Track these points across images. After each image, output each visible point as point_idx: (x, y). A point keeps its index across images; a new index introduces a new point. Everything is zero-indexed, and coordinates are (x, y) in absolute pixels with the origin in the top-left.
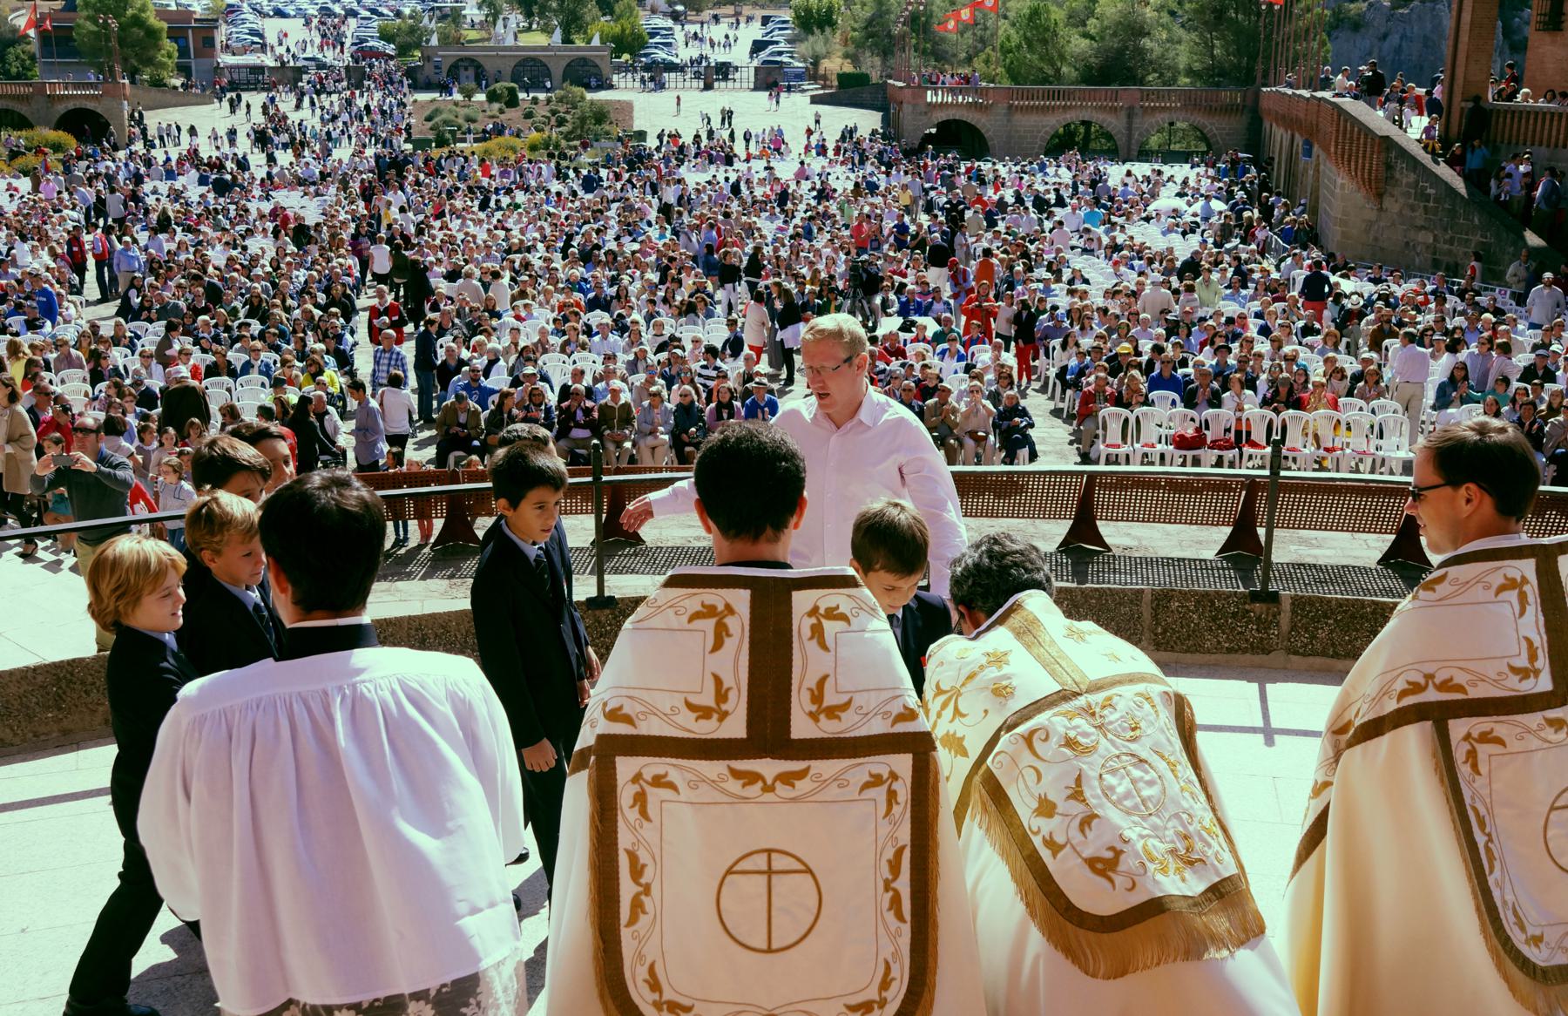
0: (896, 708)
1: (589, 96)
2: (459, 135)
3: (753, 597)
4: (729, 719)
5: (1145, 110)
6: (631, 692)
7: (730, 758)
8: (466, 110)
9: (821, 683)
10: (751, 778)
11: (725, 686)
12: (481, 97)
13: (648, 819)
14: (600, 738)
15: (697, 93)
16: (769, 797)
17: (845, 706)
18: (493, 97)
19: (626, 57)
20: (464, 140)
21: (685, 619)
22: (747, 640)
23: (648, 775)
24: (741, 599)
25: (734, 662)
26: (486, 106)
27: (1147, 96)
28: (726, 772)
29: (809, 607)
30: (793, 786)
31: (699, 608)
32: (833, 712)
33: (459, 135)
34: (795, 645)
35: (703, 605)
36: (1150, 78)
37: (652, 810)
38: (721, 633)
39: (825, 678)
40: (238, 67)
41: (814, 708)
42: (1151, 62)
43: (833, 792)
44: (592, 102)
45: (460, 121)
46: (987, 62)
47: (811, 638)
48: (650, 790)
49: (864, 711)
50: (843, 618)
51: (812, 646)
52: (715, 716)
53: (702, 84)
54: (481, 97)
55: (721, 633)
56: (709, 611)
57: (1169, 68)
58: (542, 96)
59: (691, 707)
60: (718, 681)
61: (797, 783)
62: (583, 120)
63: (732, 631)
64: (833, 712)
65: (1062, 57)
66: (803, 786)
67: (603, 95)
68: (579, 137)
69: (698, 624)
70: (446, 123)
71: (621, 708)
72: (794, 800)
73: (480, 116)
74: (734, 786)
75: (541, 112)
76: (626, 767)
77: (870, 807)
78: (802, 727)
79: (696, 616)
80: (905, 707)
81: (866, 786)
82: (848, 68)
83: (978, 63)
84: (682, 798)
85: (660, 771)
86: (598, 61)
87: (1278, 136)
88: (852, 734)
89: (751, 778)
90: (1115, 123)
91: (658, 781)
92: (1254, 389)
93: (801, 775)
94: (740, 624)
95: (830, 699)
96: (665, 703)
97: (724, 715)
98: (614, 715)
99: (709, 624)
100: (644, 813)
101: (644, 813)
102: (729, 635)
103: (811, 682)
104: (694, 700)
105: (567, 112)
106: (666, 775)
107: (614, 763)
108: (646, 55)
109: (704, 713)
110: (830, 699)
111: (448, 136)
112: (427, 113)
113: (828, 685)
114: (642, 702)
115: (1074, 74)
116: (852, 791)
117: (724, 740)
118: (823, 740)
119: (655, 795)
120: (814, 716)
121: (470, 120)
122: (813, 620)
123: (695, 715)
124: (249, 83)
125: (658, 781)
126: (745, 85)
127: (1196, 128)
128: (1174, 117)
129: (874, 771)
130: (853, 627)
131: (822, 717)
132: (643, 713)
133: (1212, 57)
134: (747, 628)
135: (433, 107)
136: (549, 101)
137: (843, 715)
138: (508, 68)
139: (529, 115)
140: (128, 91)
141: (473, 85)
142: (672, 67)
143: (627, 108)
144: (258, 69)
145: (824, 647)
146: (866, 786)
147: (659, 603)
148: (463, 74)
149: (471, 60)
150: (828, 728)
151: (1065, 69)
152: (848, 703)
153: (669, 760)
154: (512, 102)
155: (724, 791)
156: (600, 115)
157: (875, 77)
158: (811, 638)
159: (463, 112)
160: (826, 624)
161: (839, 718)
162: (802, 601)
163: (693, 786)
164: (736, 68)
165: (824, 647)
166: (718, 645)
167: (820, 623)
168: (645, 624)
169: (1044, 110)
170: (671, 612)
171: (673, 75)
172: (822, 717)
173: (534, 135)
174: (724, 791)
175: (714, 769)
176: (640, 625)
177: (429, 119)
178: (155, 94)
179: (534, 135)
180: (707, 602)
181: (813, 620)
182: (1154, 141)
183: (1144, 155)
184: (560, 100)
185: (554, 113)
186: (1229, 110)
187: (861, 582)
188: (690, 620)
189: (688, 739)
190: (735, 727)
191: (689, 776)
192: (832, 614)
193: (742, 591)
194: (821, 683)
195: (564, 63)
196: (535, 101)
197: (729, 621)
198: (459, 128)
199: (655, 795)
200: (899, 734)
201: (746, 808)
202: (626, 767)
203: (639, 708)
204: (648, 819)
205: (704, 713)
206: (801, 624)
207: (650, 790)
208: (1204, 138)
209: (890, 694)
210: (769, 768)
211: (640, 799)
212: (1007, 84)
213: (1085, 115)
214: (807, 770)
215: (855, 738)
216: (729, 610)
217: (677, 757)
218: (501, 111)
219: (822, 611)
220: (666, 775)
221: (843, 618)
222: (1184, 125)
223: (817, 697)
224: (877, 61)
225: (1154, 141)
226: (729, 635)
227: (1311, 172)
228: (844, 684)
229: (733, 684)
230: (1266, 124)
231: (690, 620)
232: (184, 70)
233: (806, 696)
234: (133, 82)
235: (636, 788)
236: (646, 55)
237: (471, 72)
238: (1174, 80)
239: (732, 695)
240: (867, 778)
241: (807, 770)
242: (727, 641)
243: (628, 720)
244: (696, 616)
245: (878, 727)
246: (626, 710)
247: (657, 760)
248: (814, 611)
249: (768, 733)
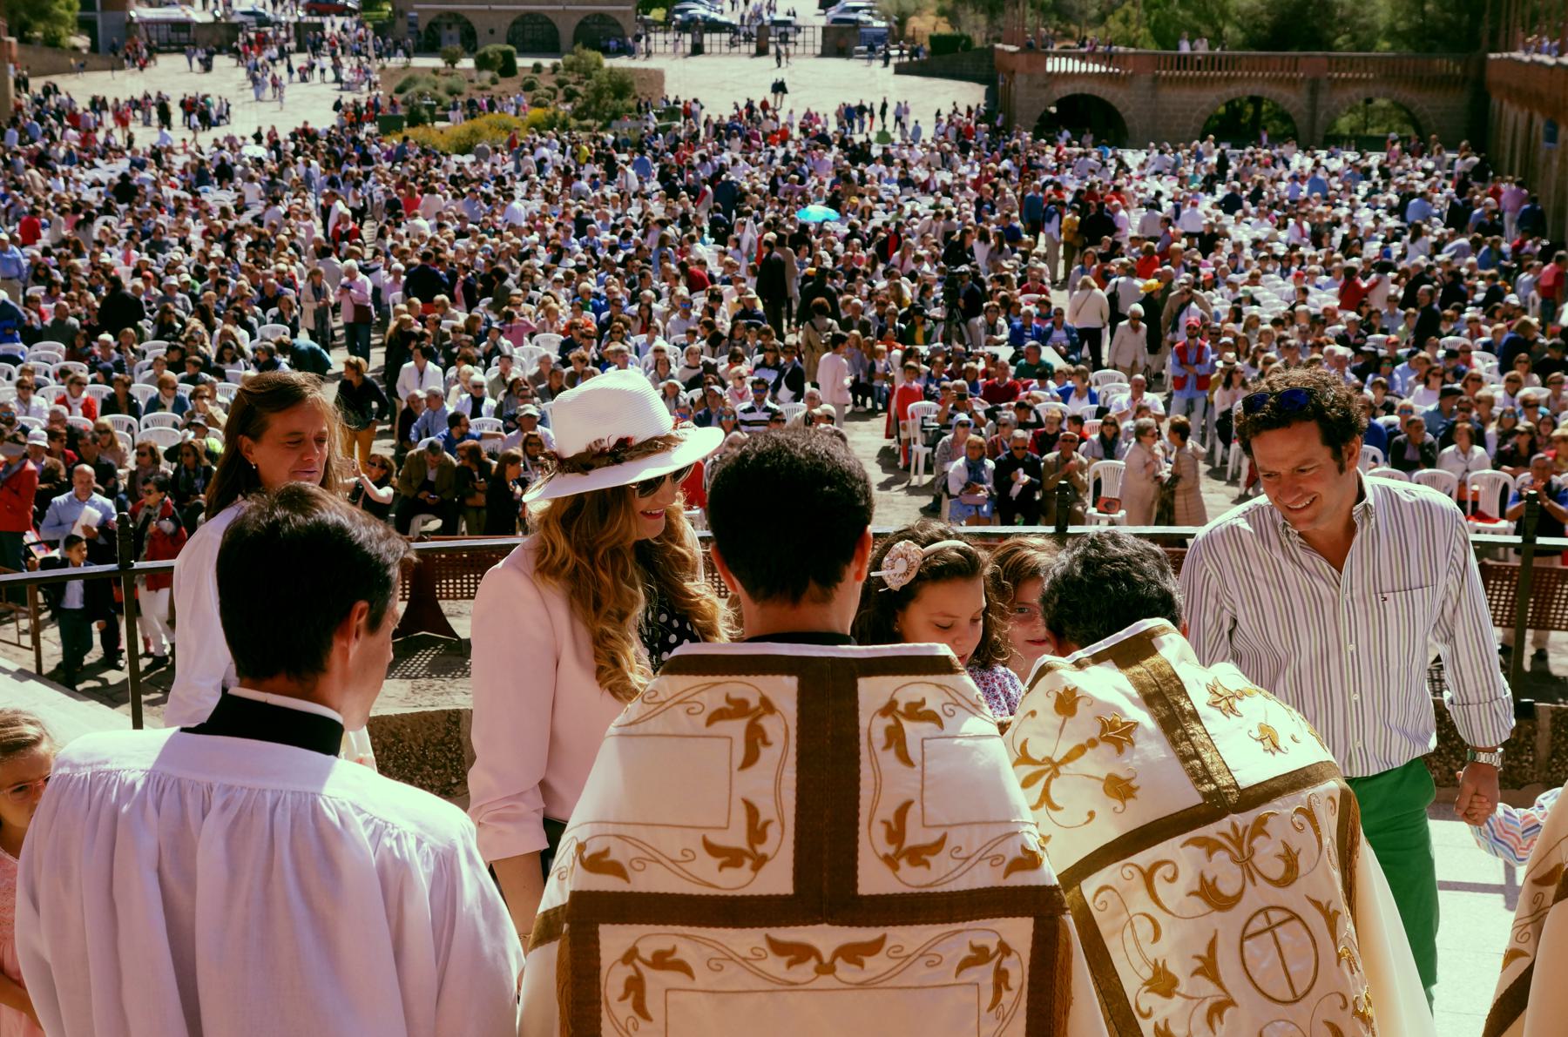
0: (1011, 851)
1: (608, 63)
2: (438, 112)
3: (801, 686)
4: (767, 867)
5: (1334, 83)
6: (623, 830)
7: (769, 925)
8: (448, 80)
9: (902, 813)
10: (800, 953)
11: (763, 818)
12: (467, 63)
13: (646, 1017)
14: (579, 898)
15: (746, 60)
16: (826, 981)
17: (939, 845)
18: (483, 63)
19: (658, 14)
20: (446, 119)
21: (702, 719)
22: (793, 750)
23: (646, 952)
24: (784, 690)
25: (774, 783)
26: (474, 75)
27: (1336, 64)
28: (764, 945)
29: (883, 702)
30: (861, 964)
31: (722, 704)
32: (918, 856)
33: (438, 112)
34: (864, 756)
35: (728, 699)
36: (1339, 41)
37: (653, 1003)
38: (755, 740)
39: (907, 805)
40: (156, 23)
41: (891, 850)
42: (1342, 22)
43: (920, 973)
44: (611, 71)
45: (441, 93)
46: (1126, 21)
47: (887, 747)
48: (649, 975)
49: (963, 853)
50: (932, 717)
51: (889, 759)
52: (748, 863)
53: (753, 49)
54: (467, 63)
55: (755, 740)
56: (738, 708)
57: (1366, 27)
58: (547, 63)
59: (712, 849)
60: (752, 811)
61: (868, 961)
62: (599, 93)
63: (770, 737)
64: (918, 856)
65: (1225, 15)
66: (876, 964)
67: (622, 62)
68: (595, 116)
69: (723, 727)
70: (421, 95)
71: (606, 852)
72: (862, 985)
73: (466, 88)
74: (775, 965)
75: (545, 83)
76: (614, 940)
77: (969, 996)
78: (873, 878)
79: (718, 716)
80: (1024, 849)
81: (966, 964)
82: (944, 29)
83: (1114, 23)
84: (699, 983)
85: (664, 944)
86: (619, 19)
87: (1512, 116)
88: (946, 888)
89: (800, 953)
90: (1293, 100)
91: (662, 961)
92: (1482, 443)
93: (874, 947)
94: (782, 727)
95: (915, 836)
96: (672, 843)
97: (760, 862)
98: (595, 863)
99: (737, 728)
100: (640, 1008)
101: (640, 1008)
102: (766, 743)
103: (887, 811)
104: (717, 839)
105: (578, 83)
106: (674, 951)
107: (596, 933)
108: (682, 11)
109: (731, 858)
110: (915, 836)
111: (424, 112)
112: (398, 82)
113: (913, 815)
114: (638, 843)
115: (1240, 36)
116: (947, 972)
117: (761, 898)
118: (902, 897)
119: (656, 981)
120: (891, 862)
121: (452, 92)
122: (889, 721)
123: (719, 861)
124: (170, 43)
125: (662, 961)
126: (809, 50)
127: (1399, 106)
128: (1372, 92)
129: (978, 942)
130: (947, 732)
131: (903, 863)
132: (639, 860)
133: (1423, 14)
134: (793, 733)
135: (405, 76)
136: (555, 68)
137: (932, 860)
138: (503, 27)
139: (529, 87)
140: (15, 51)
141: (458, 47)
142: (716, 27)
143: (657, 77)
144: (183, 25)
145: (905, 758)
146: (966, 964)
147: (662, 697)
148: (445, 34)
149: (455, 17)
150: (912, 879)
151: (1228, 30)
152: (940, 843)
153: (678, 929)
154: (509, 70)
155: (761, 974)
156: (621, 86)
157: (979, 41)
158: (887, 747)
159: (444, 81)
160: (909, 727)
161: (927, 864)
162: (872, 691)
163: (715, 966)
164: (798, 29)
165: (905, 758)
166: (750, 759)
167: (899, 725)
168: (641, 728)
169: (1202, 82)
170: (680, 710)
171: (716, 36)
172: (903, 863)
173: (536, 113)
174: (761, 974)
175: (746, 940)
176: (633, 729)
177: (400, 90)
178: (48, 55)
179: (536, 113)
180: (735, 695)
181: (889, 721)
182: (1344, 124)
183: (1333, 142)
184: (570, 68)
185: (561, 84)
186: (1444, 82)
187: (959, 665)
188: (710, 722)
189: (708, 897)
190: (777, 879)
191: (708, 951)
192: (917, 712)
193: (785, 678)
194: (902, 813)
195: (576, 21)
196: (537, 68)
197: (767, 723)
198: (439, 102)
199: (656, 981)
200: (1015, 889)
201: (792, 998)
202: (614, 940)
203: (633, 852)
204: (646, 1017)
205: (731, 858)
206: (871, 725)
207: (649, 975)
208: (1412, 120)
209: (997, 831)
210: (826, 938)
211: (635, 987)
212: (1152, 48)
213: (1255, 89)
214: (883, 939)
215: (951, 894)
216: (767, 706)
217: (690, 924)
218: (494, 82)
219: (901, 708)
220: (674, 951)
221: (932, 717)
222: (1382, 102)
223: (896, 832)
224: (982, 20)
225: (1344, 124)
226: (766, 743)
227: (1556, 163)
228: (935, 813)
229: (774, 816)
230: (1495, 101)
231: (711, 720)
232: (87, 26)
233: (880, 832)
234: (20, 41)
235: (629, 971)
236: (682, 11)
237: (455, 32)
238: (1369, 45)
239: (773, 832)
240: (967, 952)
241: (883, 939)
242: (764, 751)
243: (617, 870)
244: (718, 716)
245: (983, 877)
246: (615, 856)
247: (660, 928)
248: (890, 709)
249: (826, 886)
